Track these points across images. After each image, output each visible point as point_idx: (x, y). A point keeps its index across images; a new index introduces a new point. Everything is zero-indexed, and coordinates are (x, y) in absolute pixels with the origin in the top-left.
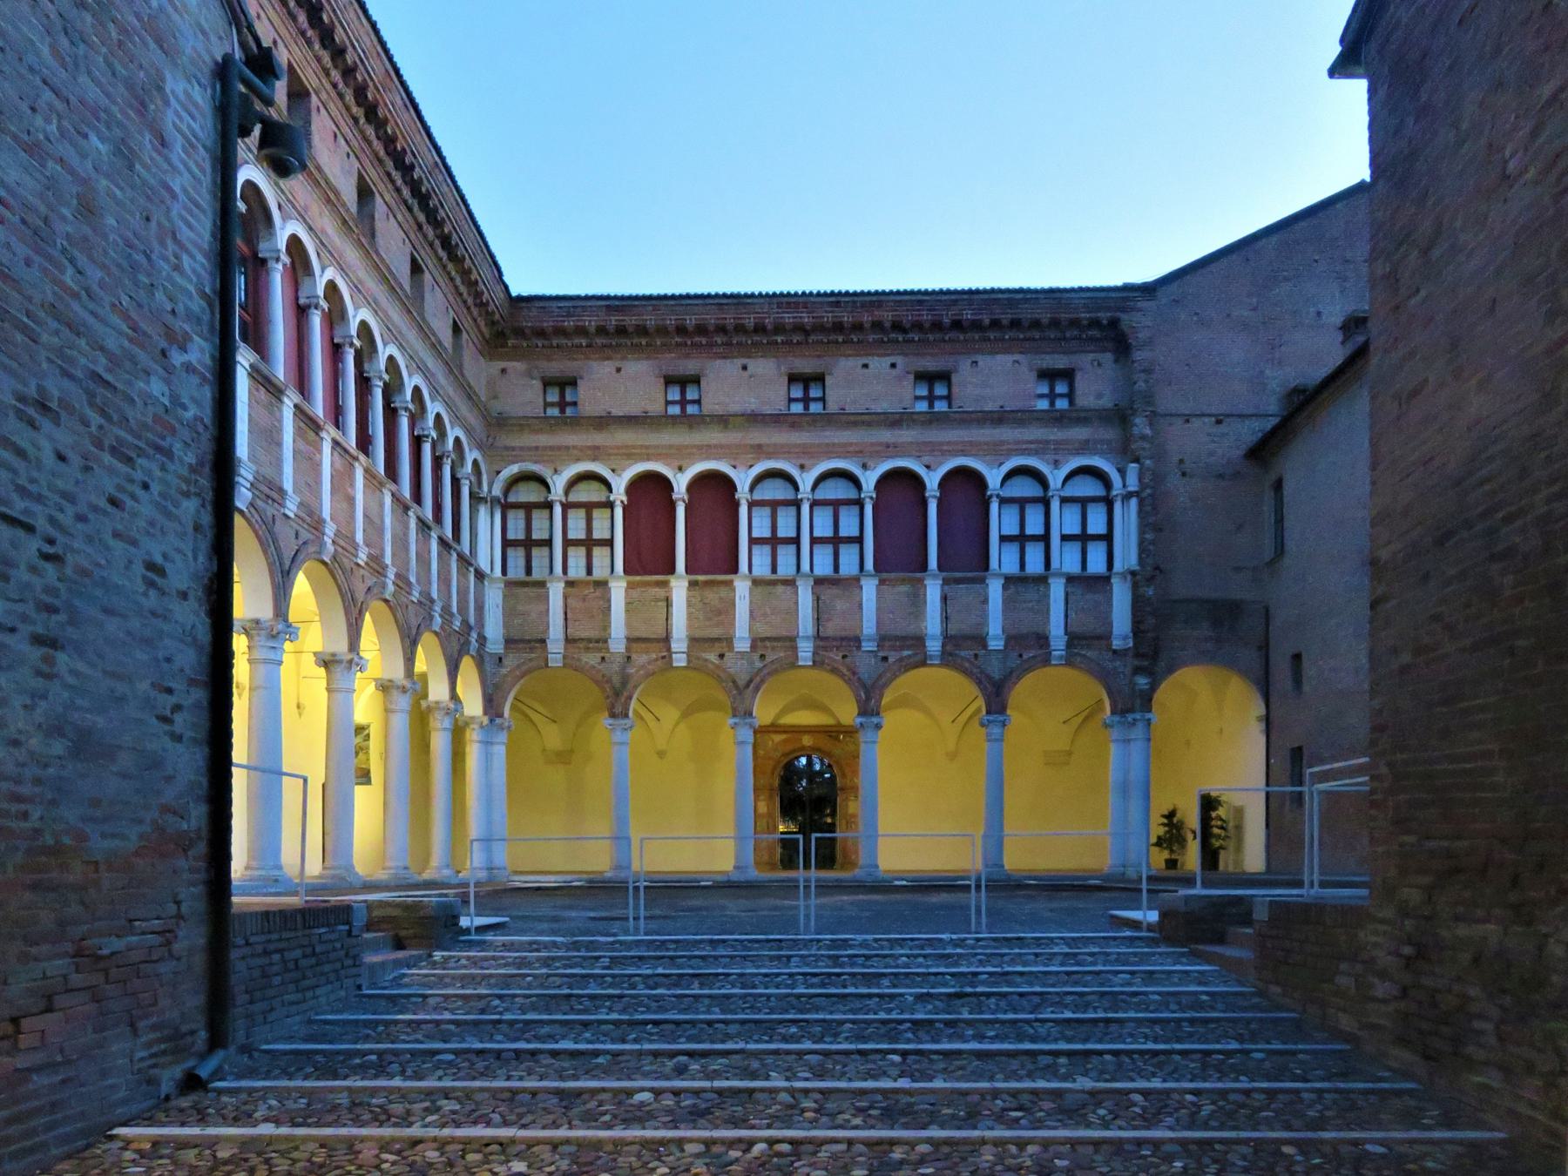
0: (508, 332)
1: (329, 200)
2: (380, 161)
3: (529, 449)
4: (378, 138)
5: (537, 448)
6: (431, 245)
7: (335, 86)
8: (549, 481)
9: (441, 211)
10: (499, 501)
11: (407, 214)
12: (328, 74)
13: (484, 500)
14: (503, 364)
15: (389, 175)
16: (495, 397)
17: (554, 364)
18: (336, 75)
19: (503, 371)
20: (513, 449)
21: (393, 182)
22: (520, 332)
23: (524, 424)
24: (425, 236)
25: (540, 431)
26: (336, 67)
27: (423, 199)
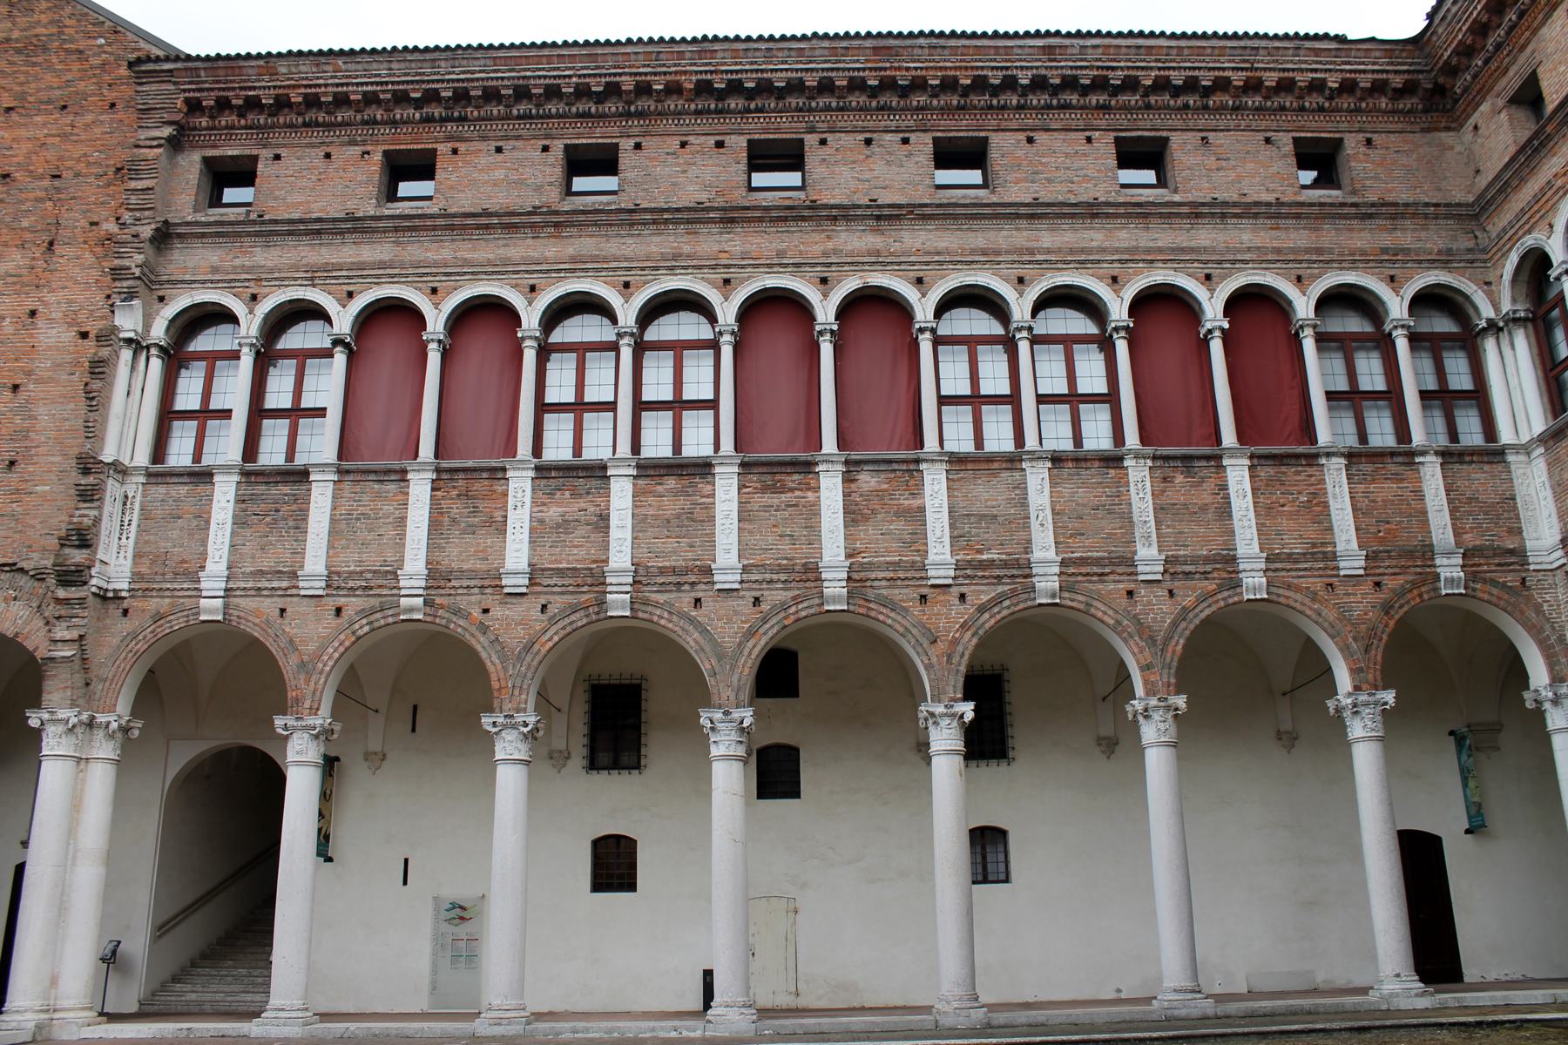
0: (1441, 80)
1: (835, 218)
2: (960, 108)
3: (1518, 218)
4: (935, 96)
5: (1523, 212)
6: (1148, 107)
7: (828, 109)
8: (1548, 249)
9: (1111, 74)
10: (1515, 320)
11: (1065, 115)
12: (810, 110)
13: (1493, 328)
14: (1472, 121)
15: (991, 107)
16: (1478, 171)
17: (1511, 73)
18: (822, 101)
19: (1476, 128)
20: (1504, 230)
21: (1004, 108)
22: (1452, 71)
23: (1507, 182)
24: (1126, 108)
25: (1523, 181)
26: (812, 98)
27: (1070, 83)
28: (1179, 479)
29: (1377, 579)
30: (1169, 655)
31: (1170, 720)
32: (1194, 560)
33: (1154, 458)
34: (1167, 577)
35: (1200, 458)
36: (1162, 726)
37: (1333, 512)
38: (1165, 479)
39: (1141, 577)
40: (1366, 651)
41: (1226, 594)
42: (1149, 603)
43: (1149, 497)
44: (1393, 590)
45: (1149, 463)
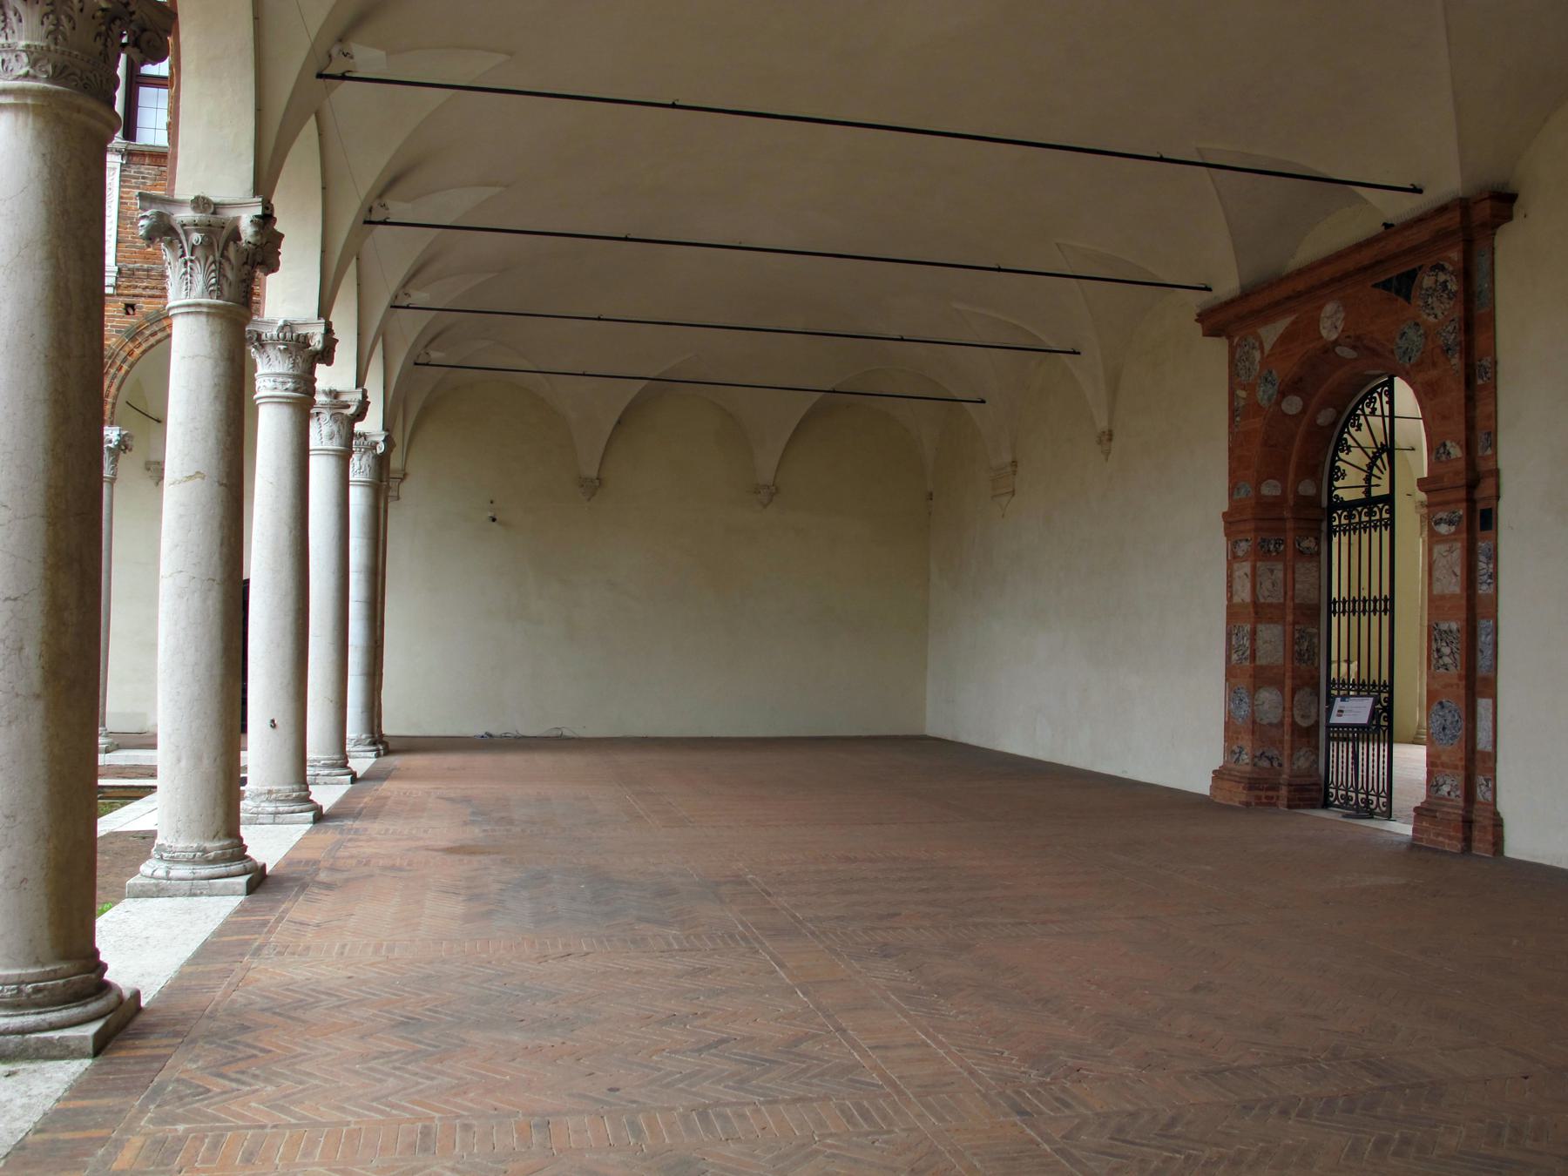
44: (146, 315)
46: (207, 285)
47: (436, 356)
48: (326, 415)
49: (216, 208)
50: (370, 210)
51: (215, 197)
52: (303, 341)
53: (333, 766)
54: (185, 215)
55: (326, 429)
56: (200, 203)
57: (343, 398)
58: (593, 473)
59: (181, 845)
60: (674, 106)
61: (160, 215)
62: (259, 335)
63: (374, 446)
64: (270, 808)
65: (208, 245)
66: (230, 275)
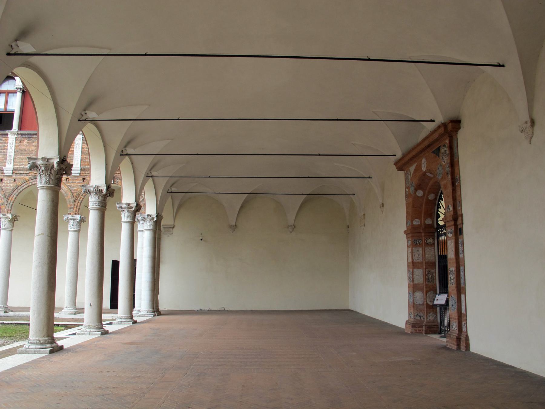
28: (26, 141)
29: (84, 177)
30: (9, 201)
31: (7, 222)
32: (23, 169)
33: (18, 134)
34: (14, 174)
35: (33, 134)
36: (4, 223)
37: (75, 154)
38: (21, 142)
39: (5, 175)
40: (75, 201)
41: (32, 181)
42: (7, 183)
43: (13, 148)
45: (16, 136)
46: (46, 181)
47: (174, 189)
48: (126, 211)
49: (48, 160)
50: (122, 151)
51: (48, 157)
52: (101, 191)
53: (127, 319)
54: (40, 162)
55: (126, 215)
56: (43, 159)
57: (131, 205)
58: (234, 224)
59: (34, 339)
60: (178, 119)
61: (33, 163)
62: (89, 190)
63: (153, 218)
64: (88, 330)
65: (46, 169)
66: (52, 178)
